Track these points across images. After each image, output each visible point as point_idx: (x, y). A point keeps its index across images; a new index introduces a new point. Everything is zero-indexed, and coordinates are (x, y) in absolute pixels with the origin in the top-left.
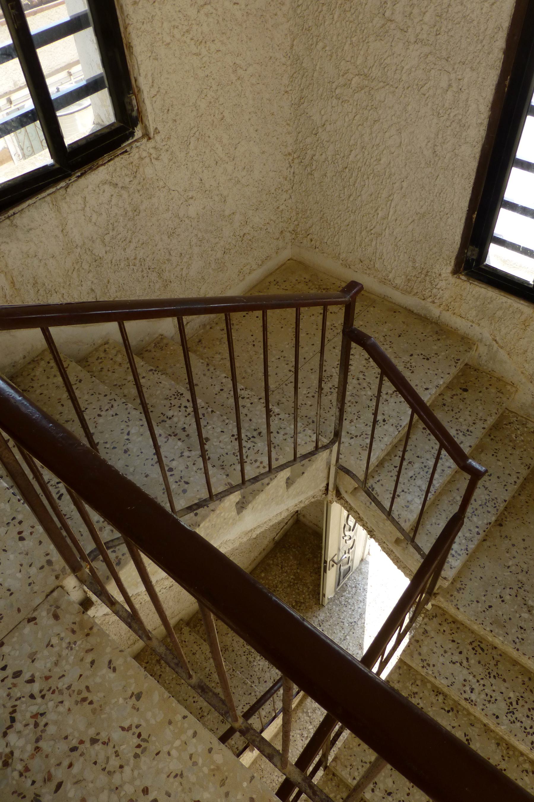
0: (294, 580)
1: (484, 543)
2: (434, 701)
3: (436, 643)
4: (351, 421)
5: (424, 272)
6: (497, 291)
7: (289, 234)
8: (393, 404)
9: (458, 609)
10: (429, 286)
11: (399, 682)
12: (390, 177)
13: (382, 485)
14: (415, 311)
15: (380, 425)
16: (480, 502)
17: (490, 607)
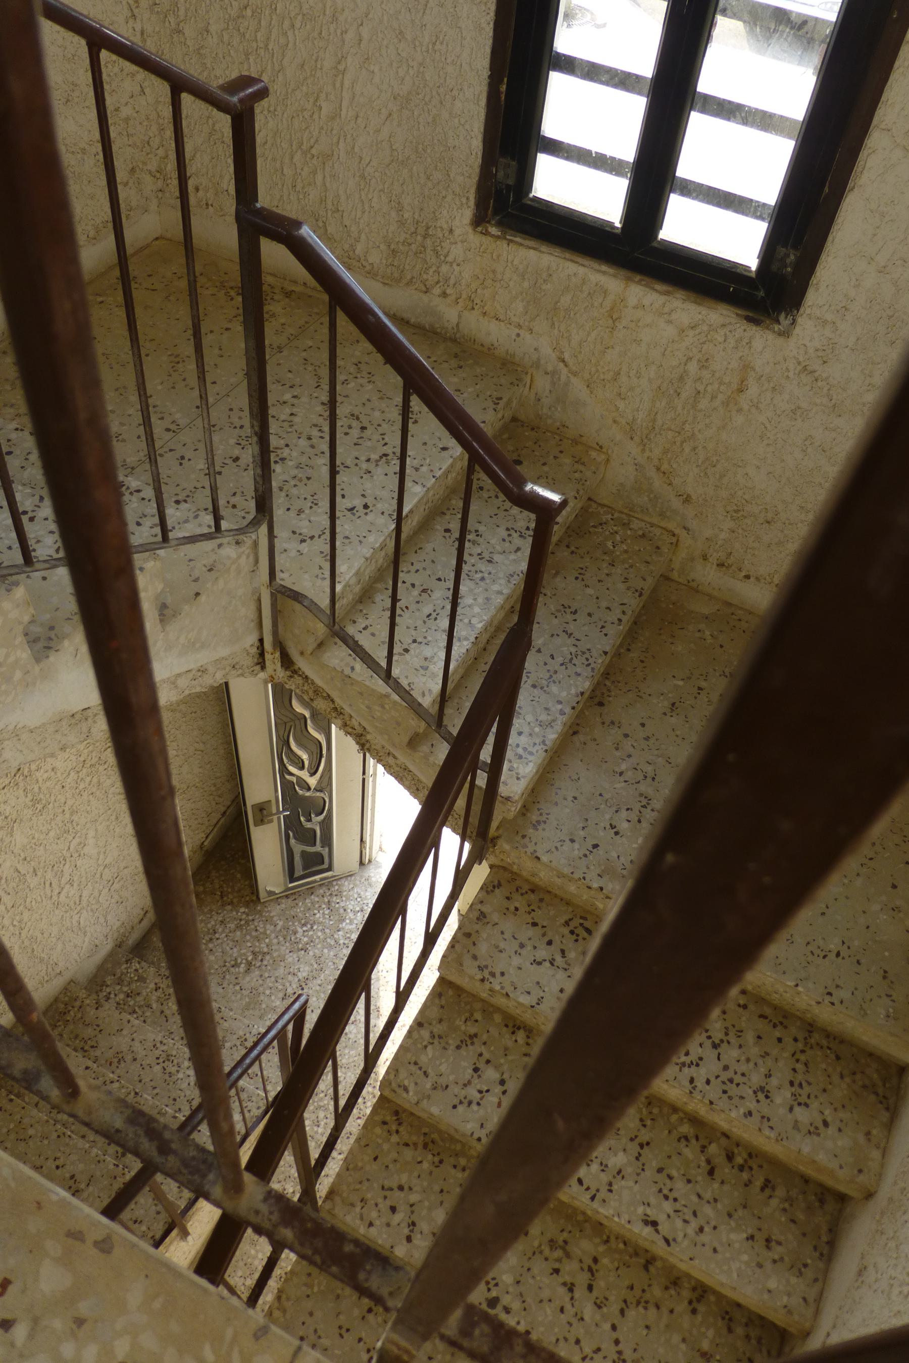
0: (248, 915)
1: (575, 738)
2: (510, 1044)
3: (502, 933)
4: (300, 512)
5: (421, 231)
6: (557, 251)
7: (148, 179)
8: (383, 477)
9: (538, 858)
10: (434, 260)
11: (440, 1021)
12: (334, 18)
13: (373, 635)
14: (412, 321)
15: (357, 514)
16: (560, 660)
17: (595, 846)
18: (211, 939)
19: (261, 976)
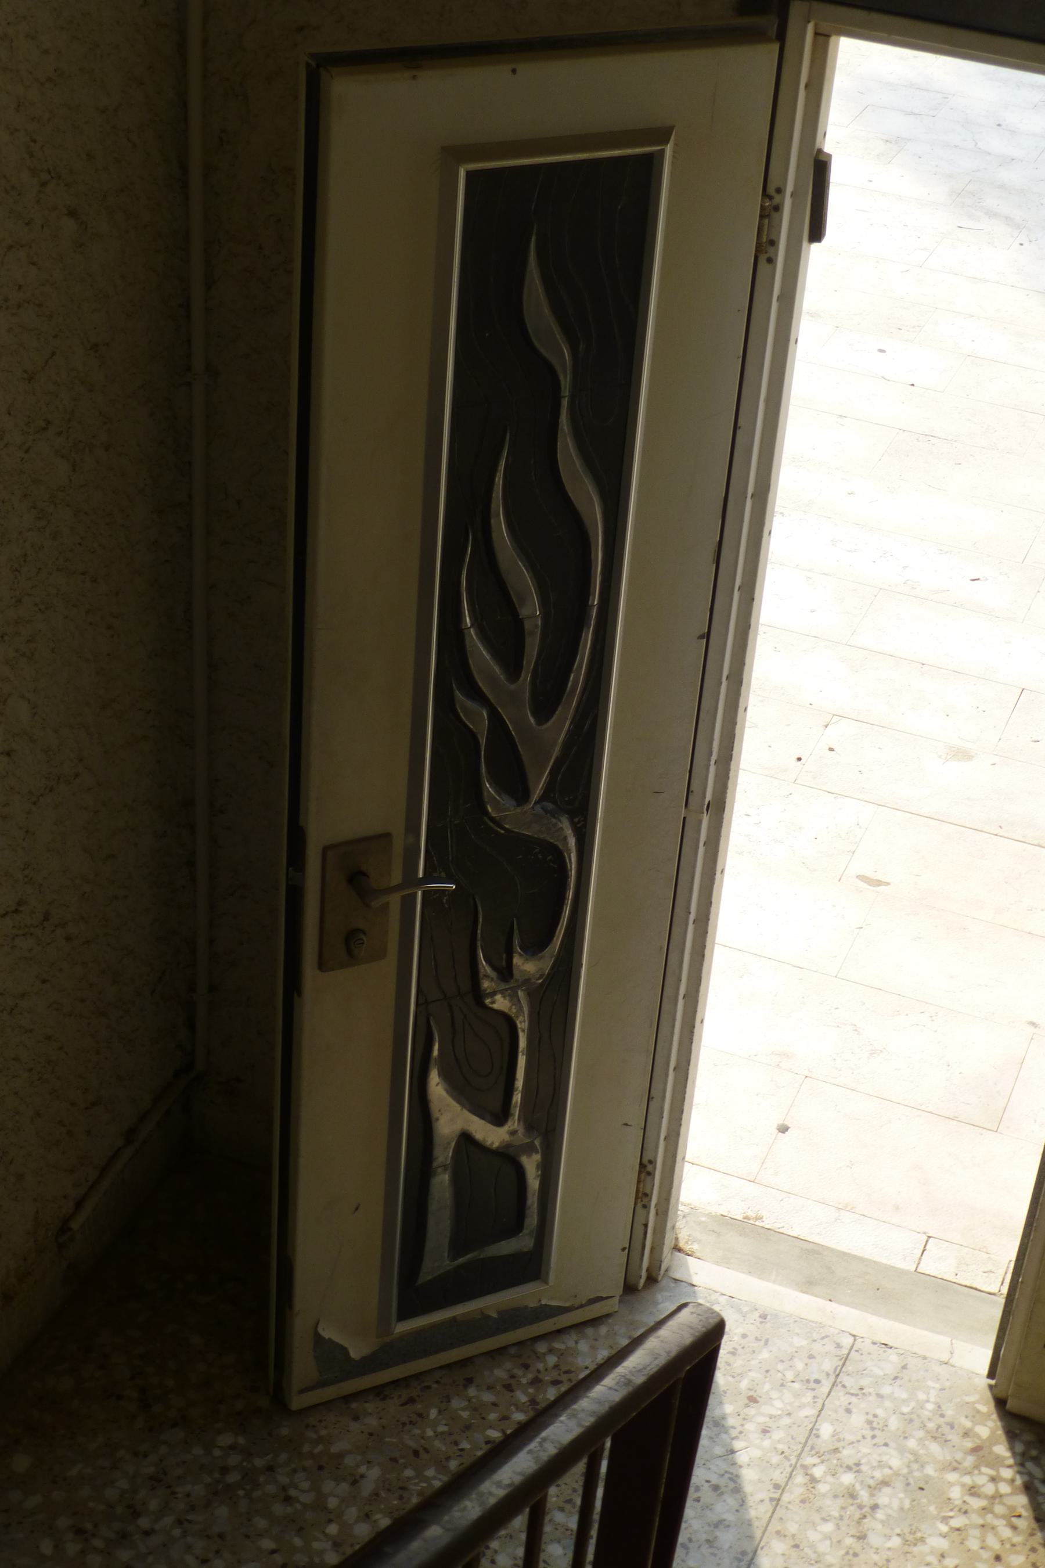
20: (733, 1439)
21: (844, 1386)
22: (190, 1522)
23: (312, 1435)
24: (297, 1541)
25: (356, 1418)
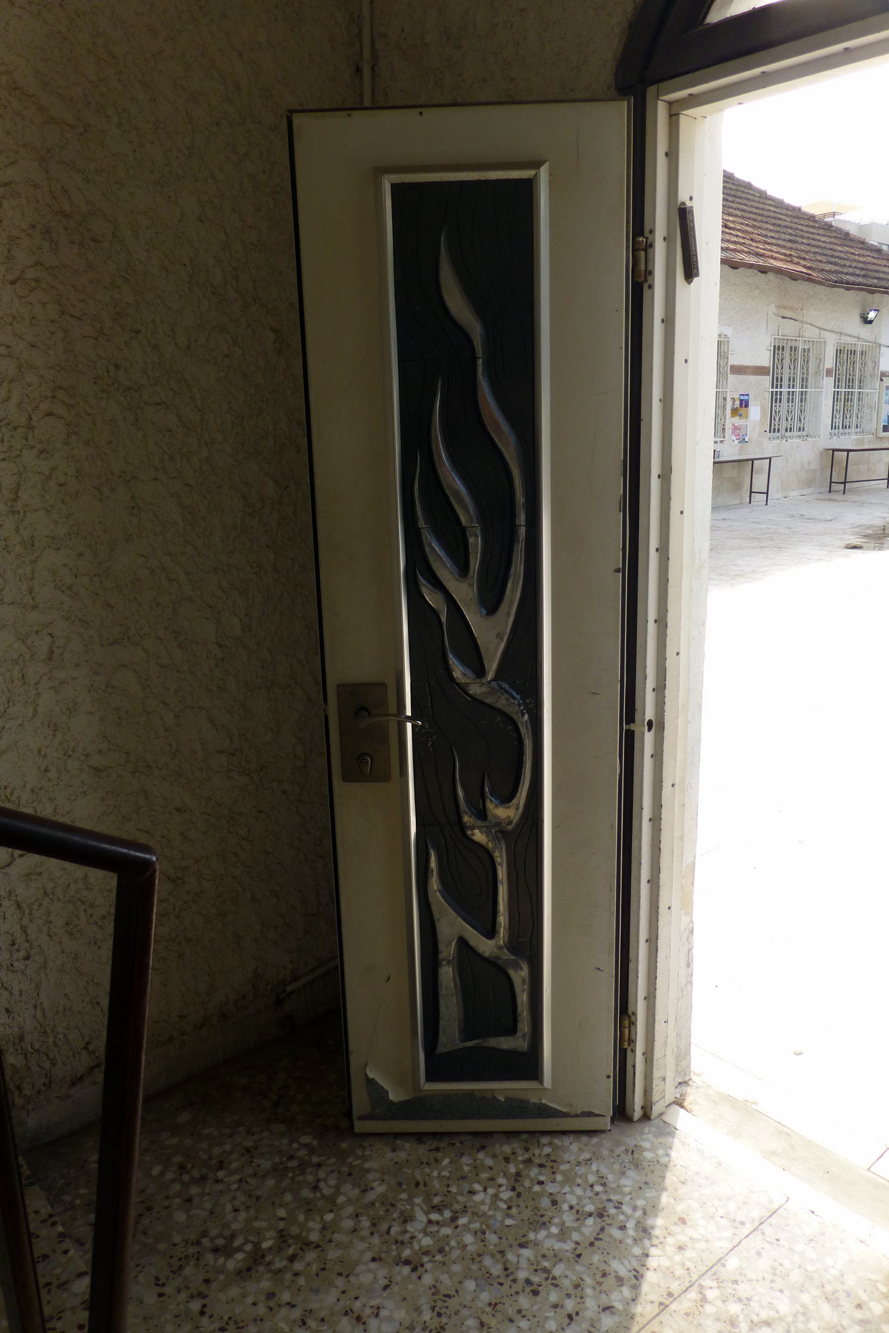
18: (203, 1178)
19: (271, 1295)
20: (652, 1246)
21: (763, 1233)
22: (247, 1182)
23: (360, 1153)
24: (301, 1218)
25: (394, 1150)
